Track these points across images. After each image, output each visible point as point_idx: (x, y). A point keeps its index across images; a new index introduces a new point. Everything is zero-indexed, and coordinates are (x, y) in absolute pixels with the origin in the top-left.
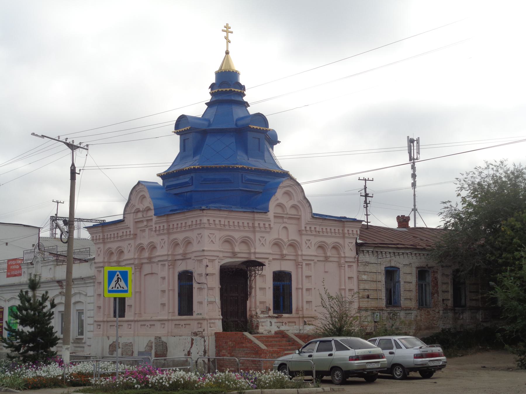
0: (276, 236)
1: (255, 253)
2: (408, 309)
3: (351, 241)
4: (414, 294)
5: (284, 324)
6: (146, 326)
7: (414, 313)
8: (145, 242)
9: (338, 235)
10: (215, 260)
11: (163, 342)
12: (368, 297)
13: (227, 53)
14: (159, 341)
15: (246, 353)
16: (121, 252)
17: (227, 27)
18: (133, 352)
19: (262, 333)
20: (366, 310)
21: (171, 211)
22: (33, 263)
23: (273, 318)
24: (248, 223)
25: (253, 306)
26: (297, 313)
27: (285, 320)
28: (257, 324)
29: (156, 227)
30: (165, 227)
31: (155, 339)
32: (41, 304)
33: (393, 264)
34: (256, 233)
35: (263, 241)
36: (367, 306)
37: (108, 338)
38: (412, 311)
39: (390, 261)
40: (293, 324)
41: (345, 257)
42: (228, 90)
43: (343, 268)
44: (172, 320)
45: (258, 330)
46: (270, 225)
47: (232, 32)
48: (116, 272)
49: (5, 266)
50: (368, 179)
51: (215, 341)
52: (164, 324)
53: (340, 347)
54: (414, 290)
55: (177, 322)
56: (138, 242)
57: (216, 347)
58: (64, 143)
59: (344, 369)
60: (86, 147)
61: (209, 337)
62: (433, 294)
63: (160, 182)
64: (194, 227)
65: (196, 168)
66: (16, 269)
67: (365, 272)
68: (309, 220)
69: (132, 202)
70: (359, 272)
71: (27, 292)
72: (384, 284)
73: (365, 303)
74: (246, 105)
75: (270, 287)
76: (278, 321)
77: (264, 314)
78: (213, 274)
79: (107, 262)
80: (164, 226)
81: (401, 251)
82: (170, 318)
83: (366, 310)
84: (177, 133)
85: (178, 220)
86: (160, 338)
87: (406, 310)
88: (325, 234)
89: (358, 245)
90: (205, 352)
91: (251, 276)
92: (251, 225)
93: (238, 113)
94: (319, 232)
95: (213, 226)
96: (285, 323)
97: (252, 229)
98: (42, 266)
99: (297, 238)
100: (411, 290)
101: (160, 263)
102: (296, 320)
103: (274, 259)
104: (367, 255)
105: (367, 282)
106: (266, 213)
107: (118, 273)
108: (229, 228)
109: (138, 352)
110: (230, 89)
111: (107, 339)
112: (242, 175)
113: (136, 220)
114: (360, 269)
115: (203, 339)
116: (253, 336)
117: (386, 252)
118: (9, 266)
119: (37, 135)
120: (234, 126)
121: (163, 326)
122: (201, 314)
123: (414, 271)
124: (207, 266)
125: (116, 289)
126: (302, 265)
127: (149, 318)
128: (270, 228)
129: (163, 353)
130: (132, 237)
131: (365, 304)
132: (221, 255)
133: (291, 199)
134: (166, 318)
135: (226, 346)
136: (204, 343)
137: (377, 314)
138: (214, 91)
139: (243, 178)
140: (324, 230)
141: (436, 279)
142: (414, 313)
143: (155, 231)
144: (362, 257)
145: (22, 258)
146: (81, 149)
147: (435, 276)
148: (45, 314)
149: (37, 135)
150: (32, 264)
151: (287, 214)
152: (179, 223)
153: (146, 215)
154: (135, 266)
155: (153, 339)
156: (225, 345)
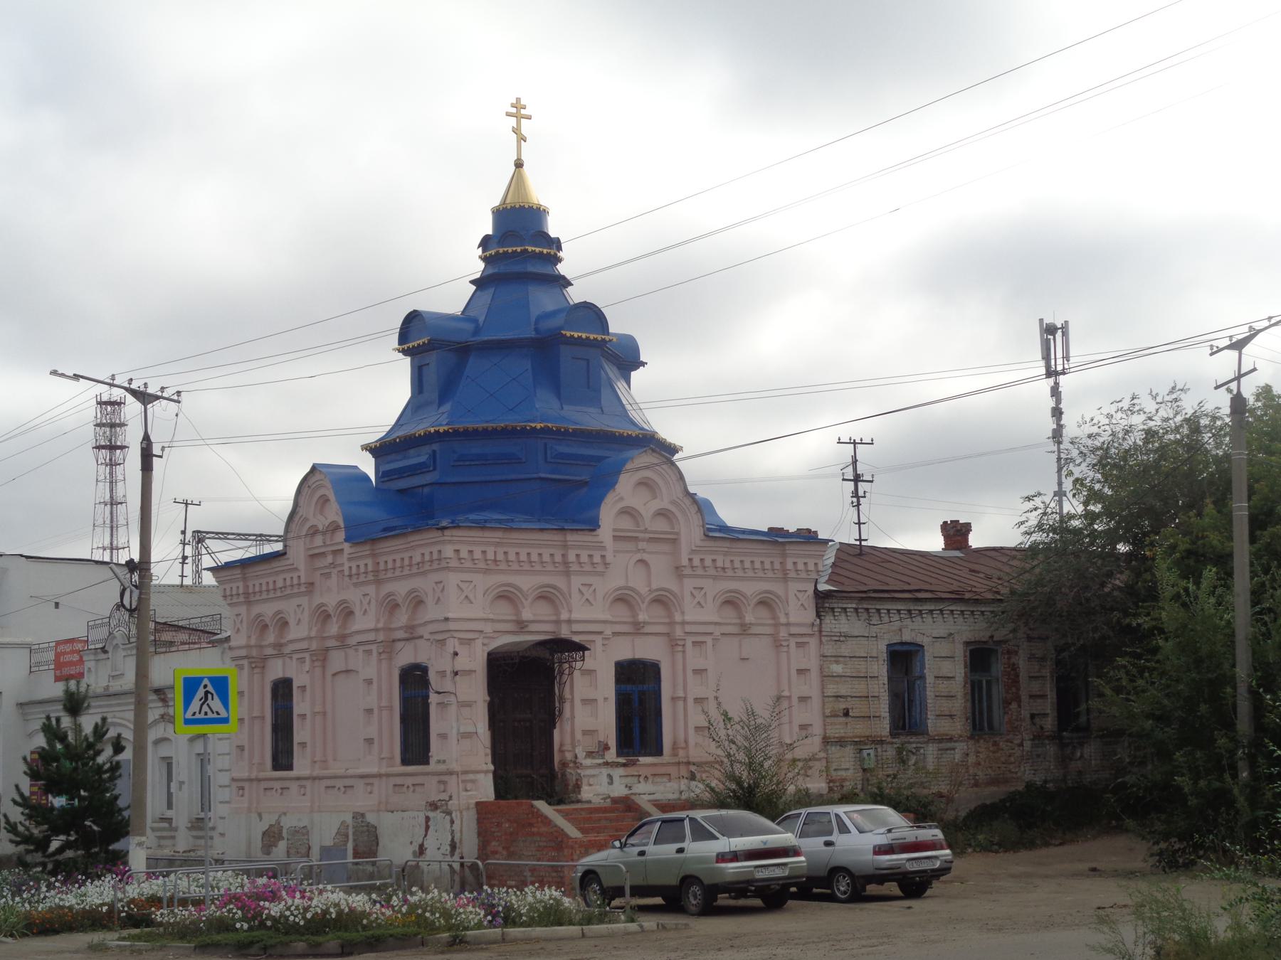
0: (621, 582)
1: (569, 622)
2: (945, 740)
3: (801, 586)
4: (959, 705)
5: (641, 779)
6: (336, 789)
7: (961, 747)
8: (331, 600)
9: (770, 574)
10: (474, 639)
12: (846, 714)
13: (519, 165)
14: (362, 822)
15: (539, 846)
16: (284, 624)
17: (518, 105)
18: (309, 848)
19: (589, 802)
20: (841, 742)
21: (385, 530)
22: (106, 648)
23: (617, 766)
24: (552, 555)
25: (568, 740)
26: (675, 755)
27: (643, 772)
28: (577, 780)
29: (350, 568)
30: (370, 568)
31: (353, 818)
32: (90, 746)
33: (907, 637)
34: (572, 577)
35: (588, 593)
36: (843, 735)
37: (260, 815)
38: (956, 744)
39: (900, 630)
40: (665, 779)
41: (788, 624)
42: (519, 249)
43: (785, 649)
44: (388, 775)
45: (580, 794)
46: (603, 557)
47: (529, 118)
48: (201, 679)
49: (51, 656)
50: (861, 440)
51: (475, 822)
53: (701, 833)
54: (960, 695)
55: (399, 781)
56: (318, 600)
57: (479, 834)
58: (126, 389)
59: (706, 881)
60: (175, 397)
61: (461, 812)
62: (1007, 703)
63: (368, 466)
64: (427, 567)
65: (441, 431)
66: (71, 664)
67: (837, 658)
68: (699, 543)
69: (301, 511)
70: (824, 656)
71: (58, 720)
72: (886, 682)
73: (837, 727)
74: (564, 282)
75: (606, 696)
76: (625, 774)
77: (594, 758)
78: (471, 672)
79: (256, 646)
80: (366, 565)
81: (925, 607)
82: (383, 771)
83: (841, 742)
84: (405, 352)
85: (396, 552)
86: (363, 815)
87: (941, 741)
88: (740, 573)
89: (821, 597)
90: (453, 846)
91: (562, 673)
92: (558, 558)
93: (543, 301)
94: (724, 569)
95: (468, 564)
96: (646, 777)
97: (561, 568)
98: (124, 656)
99: (672, 585)
100: (951, 694)
101: (361, 648)
102: (673, 771)
103: (615, 634)
104: (843, 617)
105: (843, 679)
106: (594, 530)
107: (206, 681)
108: (507, 568)
110: (522, 248)
112: (545, 445)
113: (311, 552)
114: (825, 651)
115: (448, 818)
116: (555, 810)
117: (888, 610)
118: (58, 655)
119: (63, 375)
120: (530, 333)
121: (369, 788)
122: (444, 761)
123: (959, 651)
124: (456, 654)
125: (202, 716)
126: (684, 645)
127: (341, 772)
128: (606, 565)
130: (303, 589)
131: (838, 729)
132: (488, 628)
133: (655, 497)
134: (375, 770)
135: (498, 832)
136: (451, 826)
137: (868, 751)
138: (488, 254)
139: (549, 452)
140: (737, 565)
141: (1014, 667)
142: (961, 747)
143: (350, 576)
144: (829, 623)
145: (86, 639)
146: (164, 402)
147: (1013, 660)
148: (100, 767)
149: (63, 375)
150: (104, 650)
151: (646, 531)
152: (398, 557)
153: (331, 540)
155: (349, 819)
156: (497, 830)
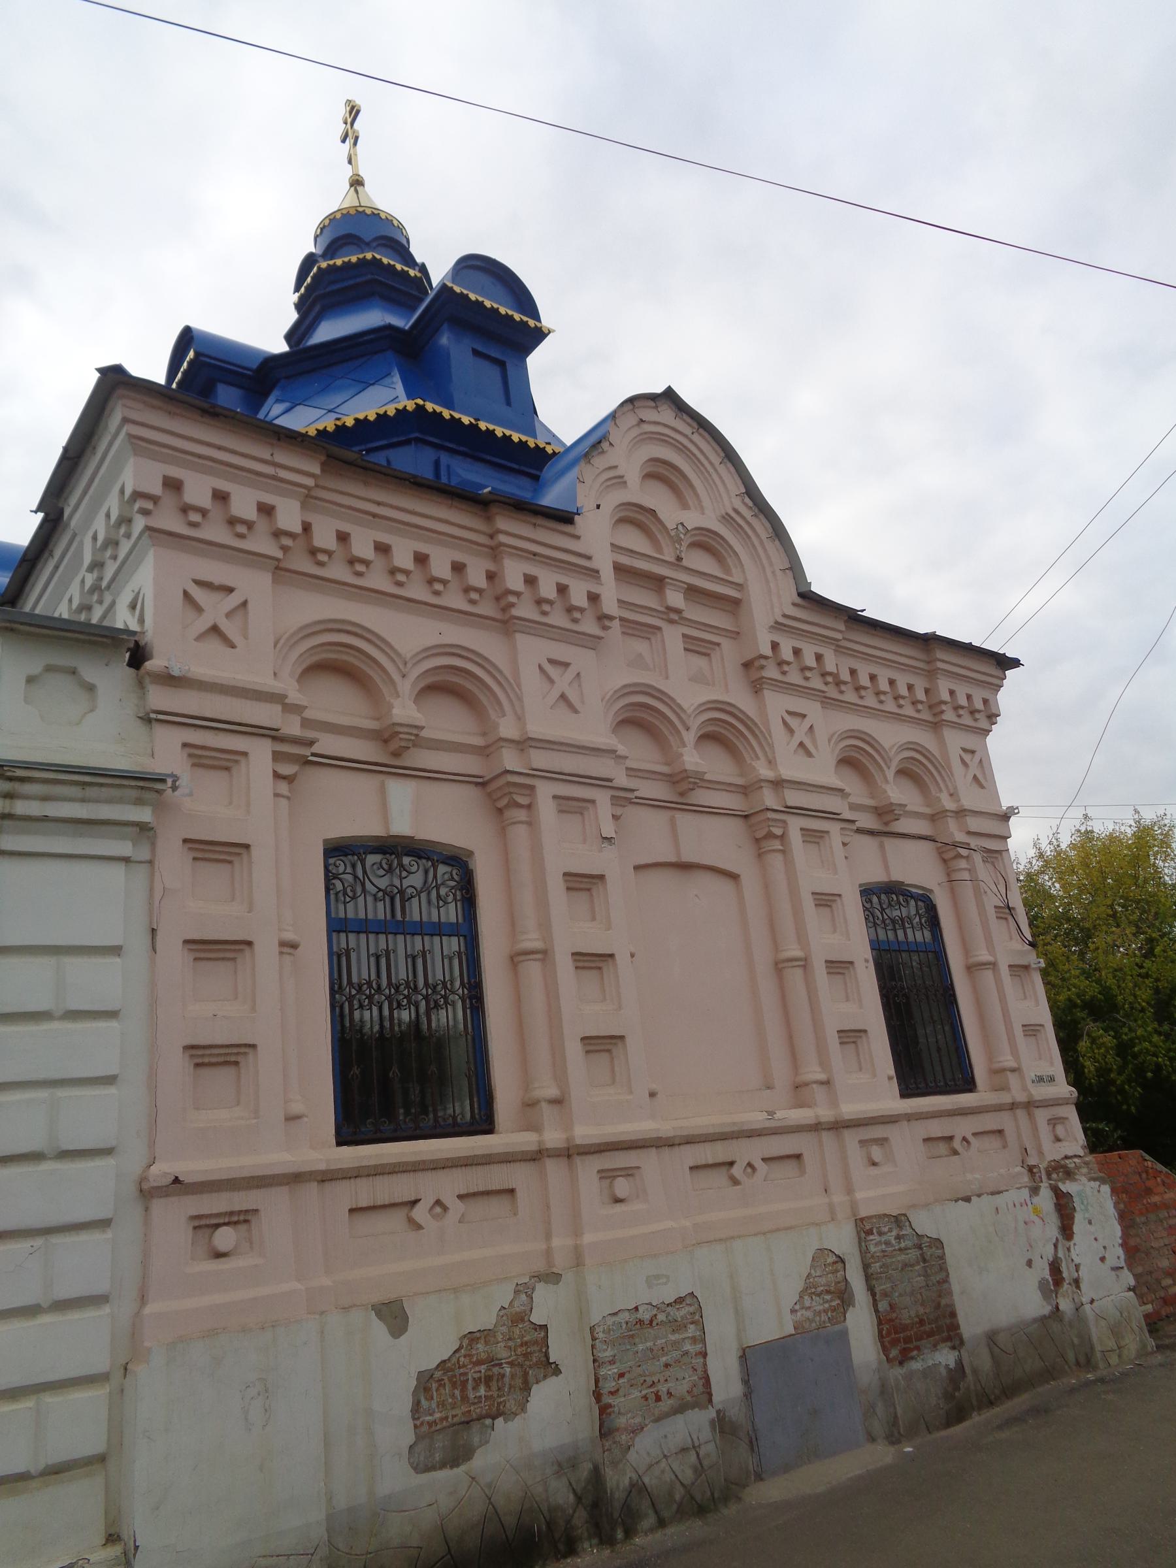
11: (921, 1242)
14: (898, 1237)
52: (882, 1142)
101: (795, 825)
109: (744, 1356)
111: (379, 1329)
129: (939, 1304)
154: (613, 797)
155: (842, 1240)
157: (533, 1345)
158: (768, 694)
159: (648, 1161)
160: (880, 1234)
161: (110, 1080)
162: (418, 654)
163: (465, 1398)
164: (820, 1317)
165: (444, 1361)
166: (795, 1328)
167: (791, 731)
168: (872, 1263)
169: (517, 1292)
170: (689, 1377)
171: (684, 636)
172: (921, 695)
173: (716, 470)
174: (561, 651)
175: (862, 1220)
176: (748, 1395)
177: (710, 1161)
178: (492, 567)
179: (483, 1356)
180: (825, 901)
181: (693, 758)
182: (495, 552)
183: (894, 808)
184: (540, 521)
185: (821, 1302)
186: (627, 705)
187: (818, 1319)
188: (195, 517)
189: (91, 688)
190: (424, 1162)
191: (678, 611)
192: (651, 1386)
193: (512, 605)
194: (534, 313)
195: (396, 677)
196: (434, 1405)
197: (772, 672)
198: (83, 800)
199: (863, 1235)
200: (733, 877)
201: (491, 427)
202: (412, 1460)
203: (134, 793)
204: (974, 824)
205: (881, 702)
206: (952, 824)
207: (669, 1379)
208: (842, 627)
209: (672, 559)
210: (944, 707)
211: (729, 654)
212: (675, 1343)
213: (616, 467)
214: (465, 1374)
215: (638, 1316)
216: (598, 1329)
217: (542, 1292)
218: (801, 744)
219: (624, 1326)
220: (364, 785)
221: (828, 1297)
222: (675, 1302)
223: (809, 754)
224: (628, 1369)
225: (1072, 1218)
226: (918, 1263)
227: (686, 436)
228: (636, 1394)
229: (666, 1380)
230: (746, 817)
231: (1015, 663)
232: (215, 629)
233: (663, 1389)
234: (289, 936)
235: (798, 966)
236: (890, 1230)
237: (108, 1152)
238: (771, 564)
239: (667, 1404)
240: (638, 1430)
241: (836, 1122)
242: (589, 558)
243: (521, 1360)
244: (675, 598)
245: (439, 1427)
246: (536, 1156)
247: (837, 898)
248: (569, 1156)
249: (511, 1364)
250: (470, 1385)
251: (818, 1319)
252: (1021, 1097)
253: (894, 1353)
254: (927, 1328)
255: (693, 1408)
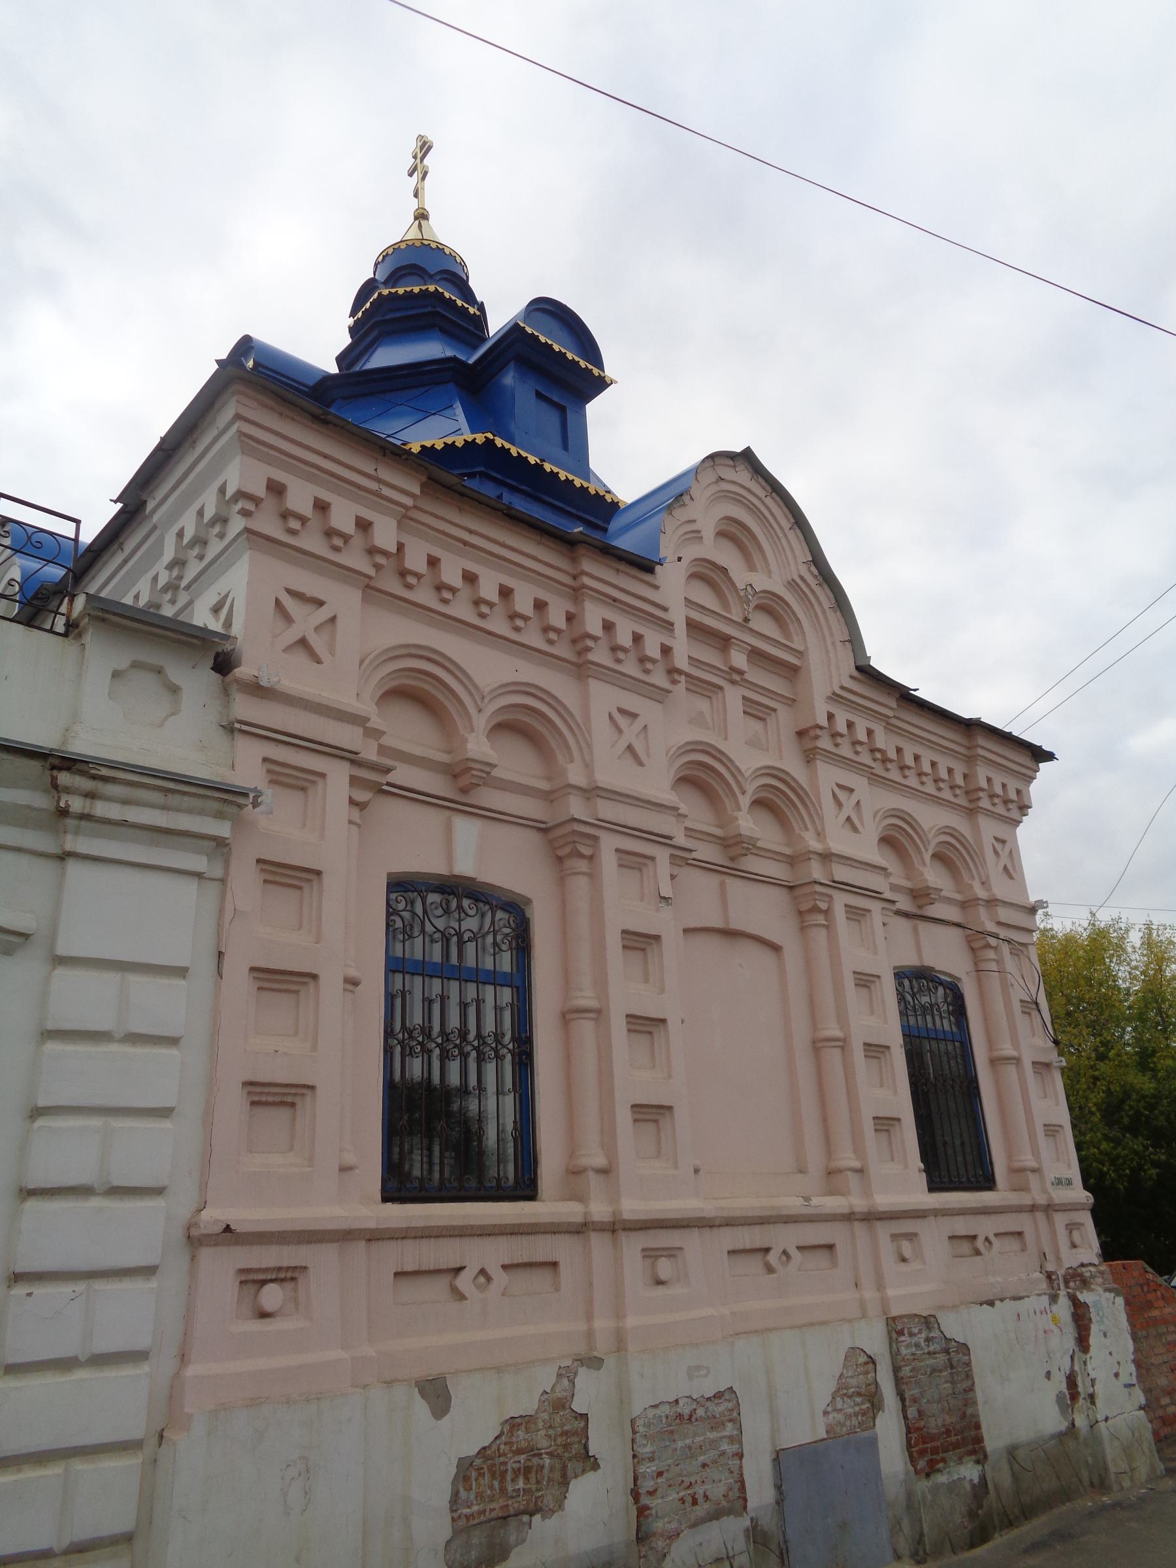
14: (928, 1340)
52: (912, 1237)
101: (841, 900)
109: (777, 1460)
111: (421, 1408)
129: (964, 1416)
154: (672, 856)
155: (874, 1340)
157: (573, 1435)
158: (821, 767)
159: (691, 1242)
160: (911, 1335)
161: (164, 1113)
162: (495, 689)
163: (503, 1490)
164: (851, 1421)
165: (484, 1448)
166: (827, 1432)
167: (839, 804)
168: (903, 1366)
169: (559, 1376)
170: (726, 1479)
171: (744, 698)
172: (959, 781)
173: (785, 535)
174: (632, 702)
175: (894, 1319)
176: (779, 1502)
177: (748, 1247)
178: (572, 610)
179: (524, 1444)
180: (865, 981)
181: (748, 823)
182: (577, 593)
183: (930, 891)
184: (623, 567)
185: (853, 1404)
186: (688, 763)
187: (848, 1423)
188: (294, 524)
189: (174, 690)
190: (472, 1227)
191: (741, 673)
192: (688, 1487)
193: (589, 649)
194: (597, 360)
195: (472, 710)
196: (472, 1497)
197: (825, 743)
198: (164, 808)
199: (894, 1335)
200: (776, 948)
201: (556, 470)
202: (447, 1557)
203: (216, 805)
204: (1004, 914)
205: (923, 783)
206: (983, 913)
207: (705, 1480)
208: (893, 704)
209: (740, 620)
210: (981, 794)
211: (785, 721)
212: (712, 1442)
213: (694, 521)
214: (505, 1463)
215: (679, 1410)
216: (640, 1422)
217: (584, 1377)
218: (849, 819)
219: (664, 1420)
220: (431, 819)
221: (858, 1400)
222: (714, 1396)
223: (855, 829)
224: (667, 1468)
225: (1088, 1329)
226: (946, 1369)
227: (759, 499)
228: (673, 1496)
229: (703, 1482)
230: (791, 888)
231: (1049, 756)
232: (303, 642)
233: (700, 1490)
234: (353, 973)
235: (838, 1047)
236: (920, 1332)
237: (158, 1191)
238: (832, 635)
239: (702, 1509)
240: (675, 1535)
241: (870, 1213)
242: (665, 609)
243: (560, 1451)
244: (739, 659)
245: (476, 1521)
246: (581, 1229)
247: (876, 979)
248: (614, 1231)
249: (550, 1454)
250: (509, 1477)
251: (848, 1423)
252: (1041, 1200)
253: (922, 1464)
254: (953, 1439)
255: (728, 1514)
